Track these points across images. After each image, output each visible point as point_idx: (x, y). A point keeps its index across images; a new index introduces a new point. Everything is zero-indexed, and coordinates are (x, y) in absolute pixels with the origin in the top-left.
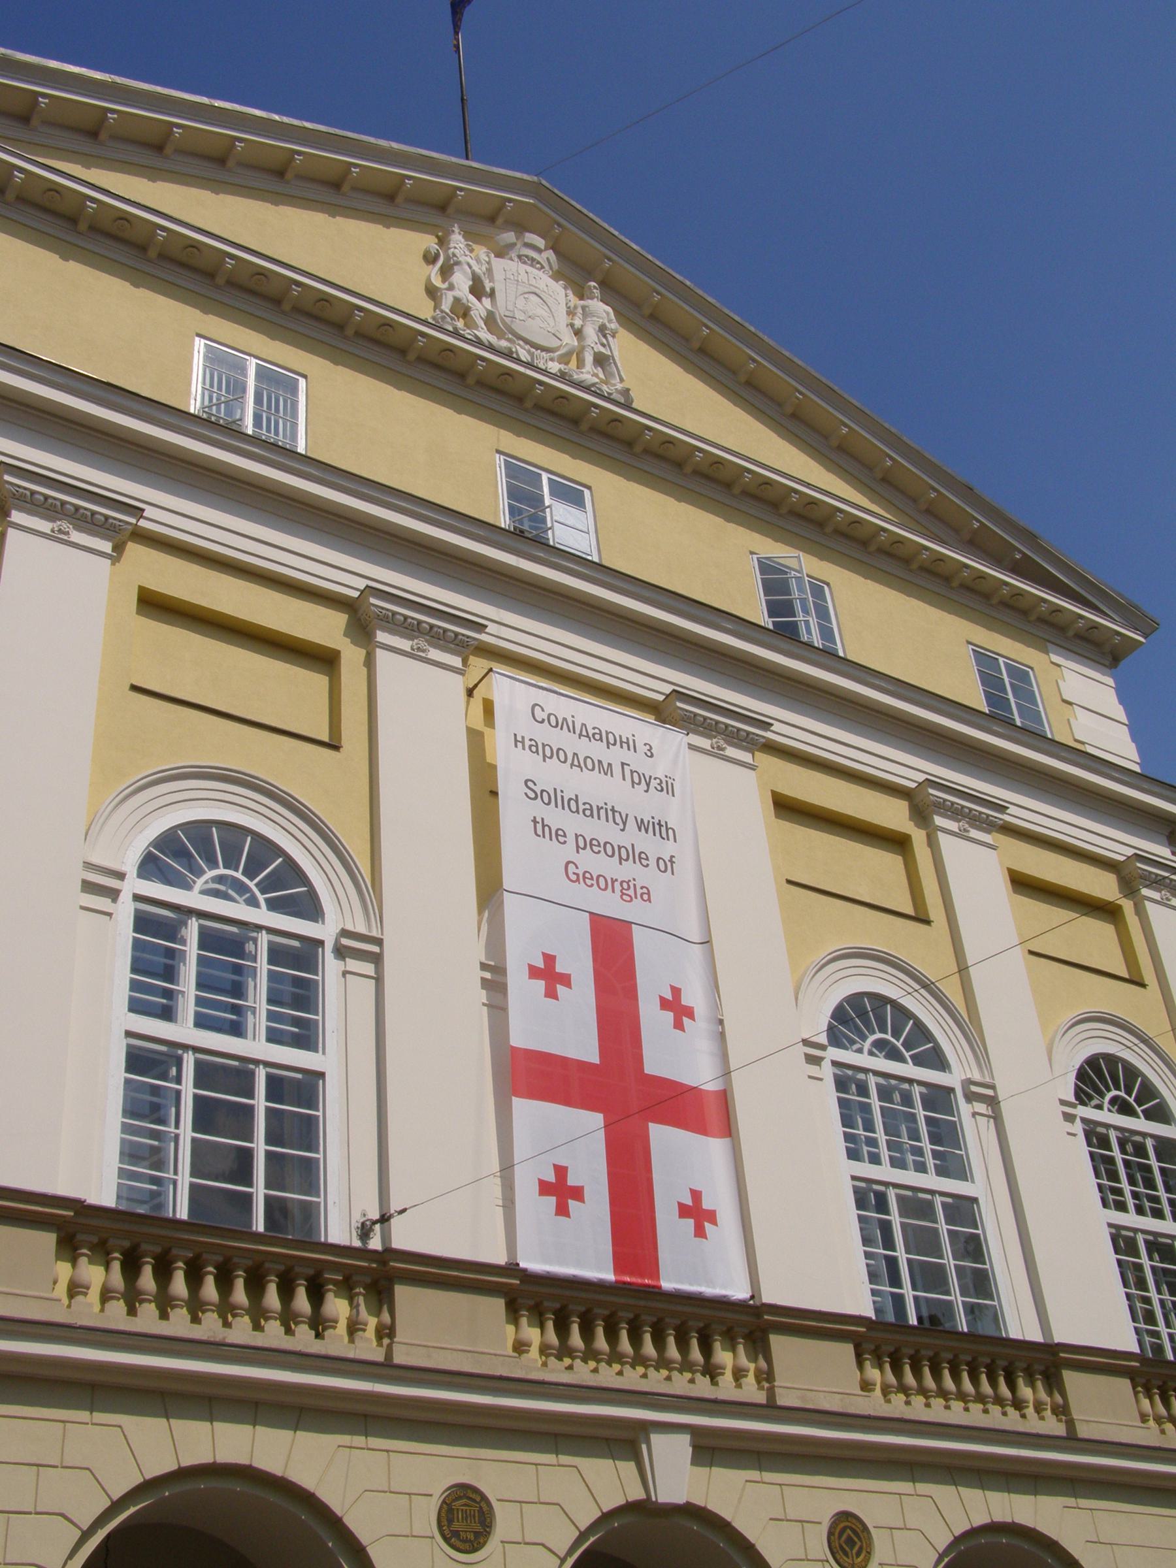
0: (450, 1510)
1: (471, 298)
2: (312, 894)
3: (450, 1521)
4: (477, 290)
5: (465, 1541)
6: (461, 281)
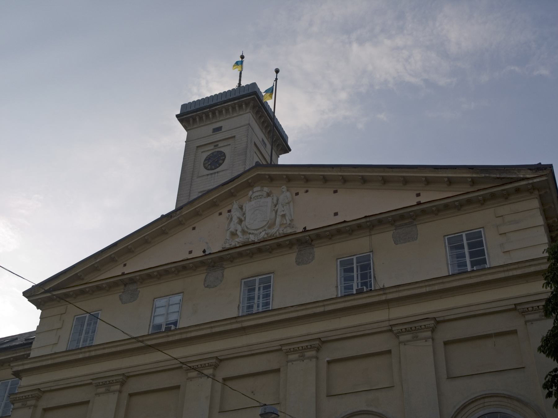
4: (240, 221)
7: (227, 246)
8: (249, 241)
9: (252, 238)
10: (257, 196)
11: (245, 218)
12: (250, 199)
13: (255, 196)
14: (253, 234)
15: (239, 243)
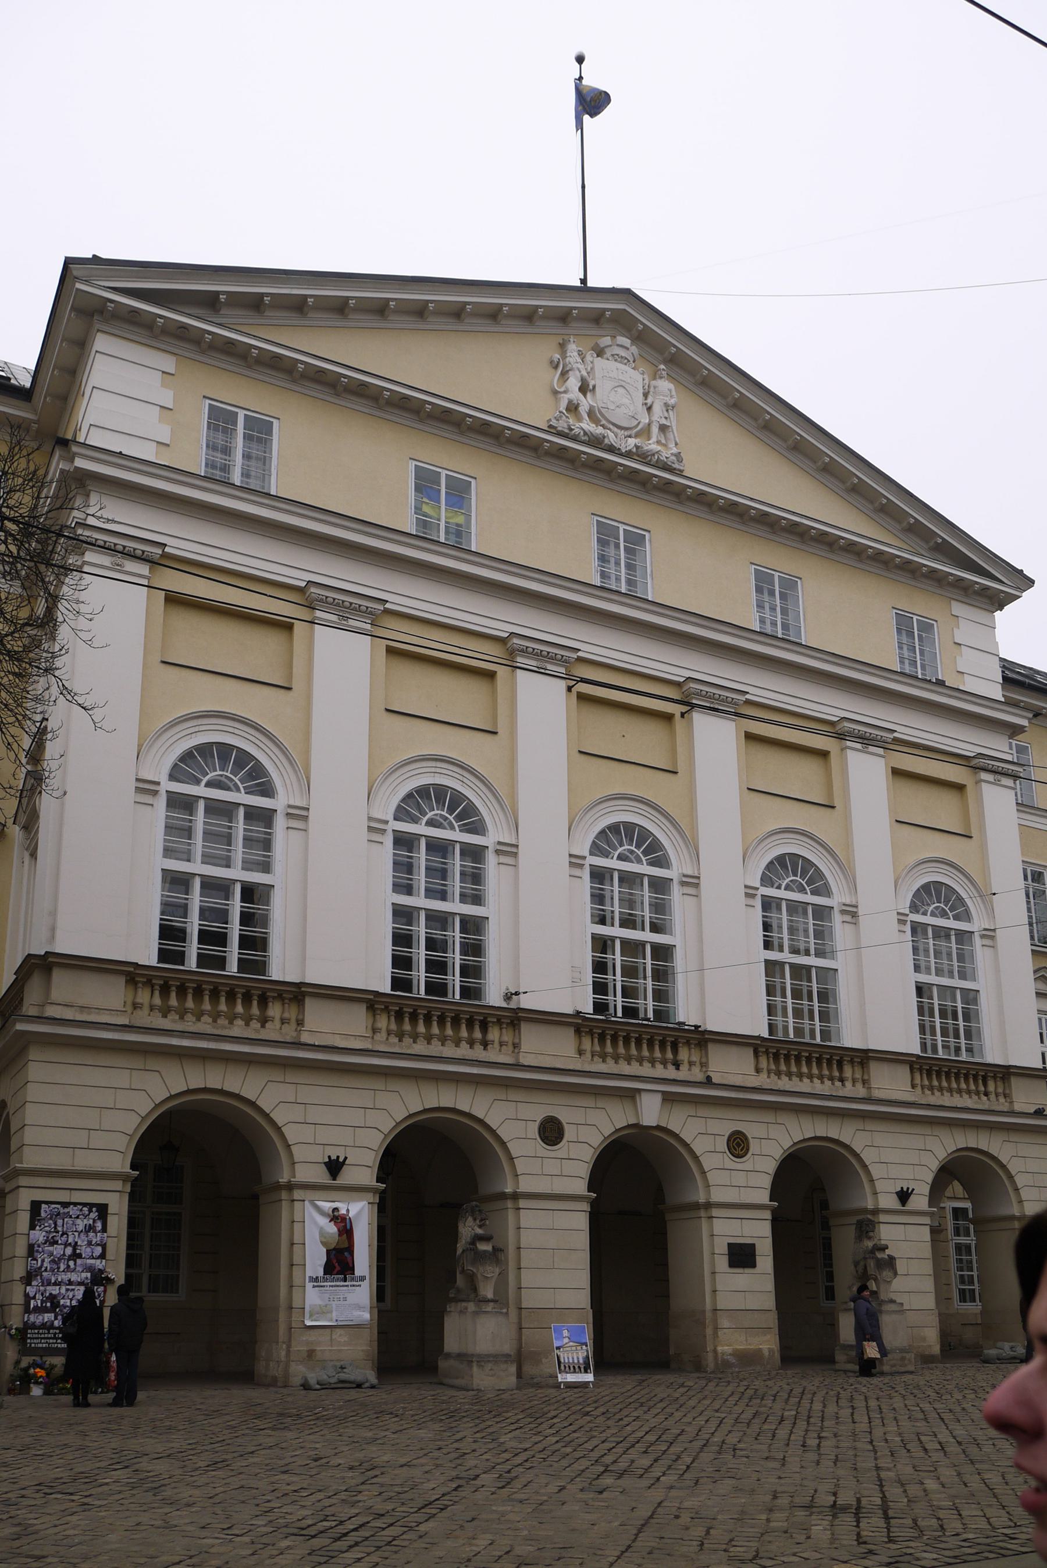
0: (544, 1127)
1: (581, 396)
2: (482, 821)
3: (544, 1132)
4: (584, 389)
5: (551, 1141)
6: (573, 383)
7: (562, 426)
8: (603, 441)
9: (611, 438)
10: (622, 357)
11: (594, 387)
12: (600, 353)
13: (618, 355)
14: (609, 429)
15: (585, 433)
